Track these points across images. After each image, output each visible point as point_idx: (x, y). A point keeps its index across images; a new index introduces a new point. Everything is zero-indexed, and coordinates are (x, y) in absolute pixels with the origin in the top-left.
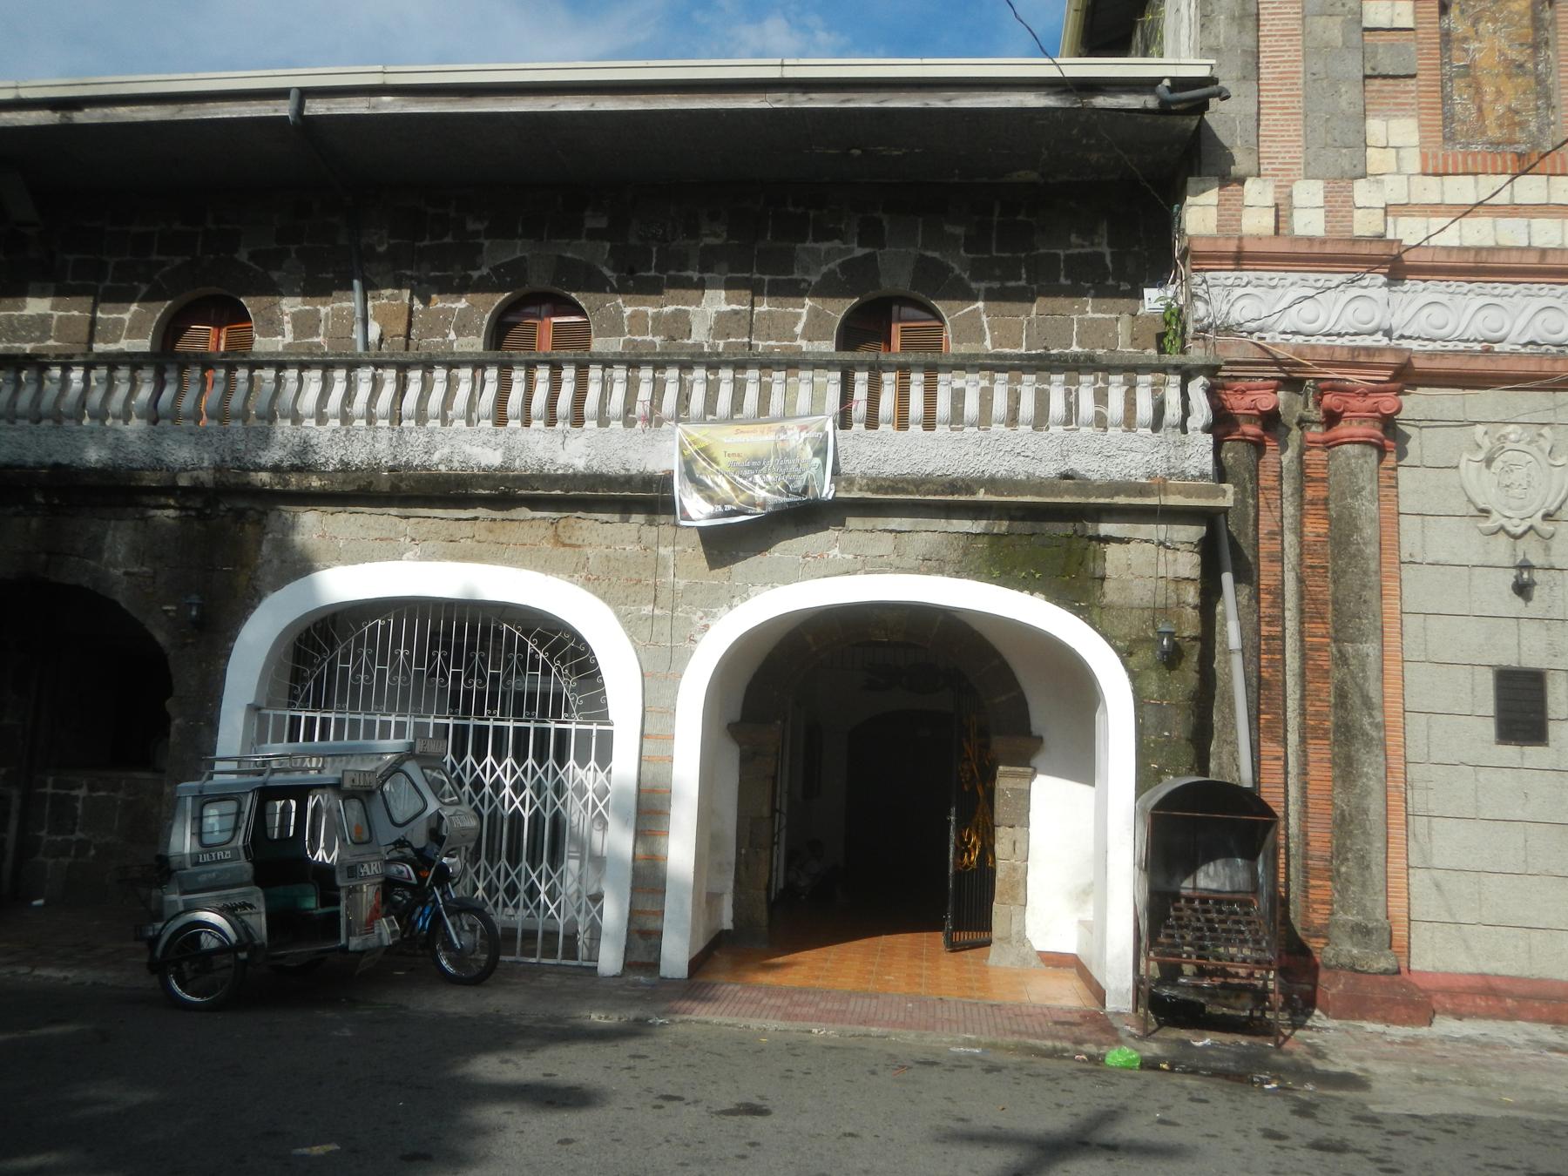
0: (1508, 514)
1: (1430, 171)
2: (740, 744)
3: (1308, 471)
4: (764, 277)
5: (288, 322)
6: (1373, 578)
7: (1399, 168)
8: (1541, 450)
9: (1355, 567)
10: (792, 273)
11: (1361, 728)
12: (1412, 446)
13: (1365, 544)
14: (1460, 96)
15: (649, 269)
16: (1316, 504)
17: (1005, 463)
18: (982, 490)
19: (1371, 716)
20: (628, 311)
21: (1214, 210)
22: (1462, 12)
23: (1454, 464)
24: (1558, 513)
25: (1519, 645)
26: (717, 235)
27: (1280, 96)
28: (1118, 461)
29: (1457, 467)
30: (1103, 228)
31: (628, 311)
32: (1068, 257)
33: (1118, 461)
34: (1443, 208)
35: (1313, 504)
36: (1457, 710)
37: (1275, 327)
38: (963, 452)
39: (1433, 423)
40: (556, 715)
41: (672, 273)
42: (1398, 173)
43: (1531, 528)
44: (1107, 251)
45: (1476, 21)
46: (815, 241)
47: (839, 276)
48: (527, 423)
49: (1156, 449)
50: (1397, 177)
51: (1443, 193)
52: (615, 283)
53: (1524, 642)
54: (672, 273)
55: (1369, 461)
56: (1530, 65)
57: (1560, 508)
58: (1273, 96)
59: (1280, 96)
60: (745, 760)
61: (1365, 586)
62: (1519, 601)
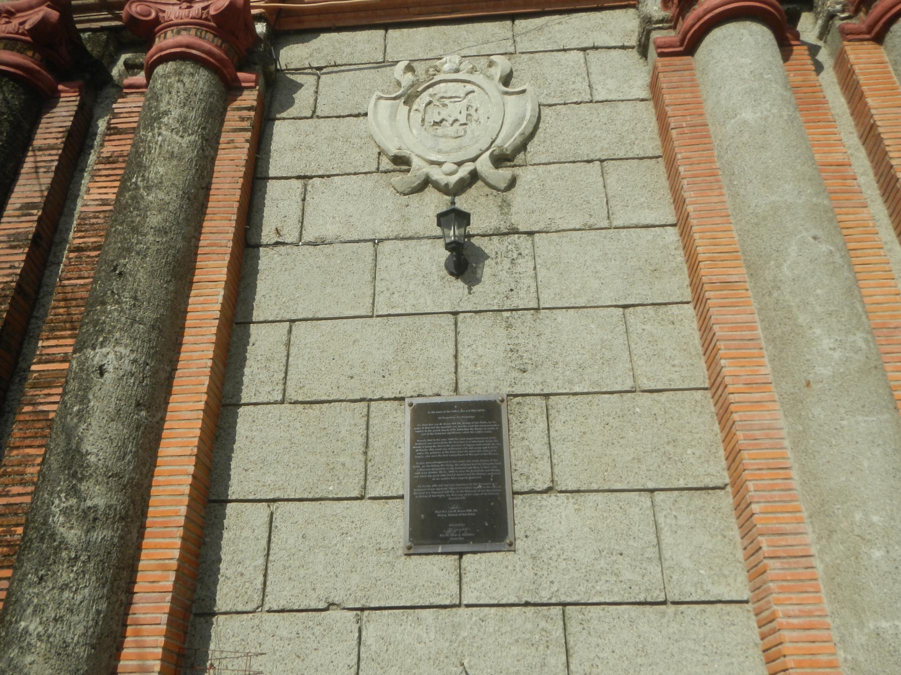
0: (434, 157)
3: (113, 121)
6: (150, 238)
8: (490, 77)
9: (121, 224)
11: (45, 523)
12: (303, 99)
13: (148, 188)
16: (114, 163)
19: (74, 491)
23: (362, 112)
24: (521, 156)
25: (456, 357)
29: (366, 114)
35: (110, 163)
36: (332, 489)
39: (336, 67)
43: (474, 176)
53: (464, 352)
55: (186, 80)
57: (522, 147)
61: (129, 250)
62: (459, 286)
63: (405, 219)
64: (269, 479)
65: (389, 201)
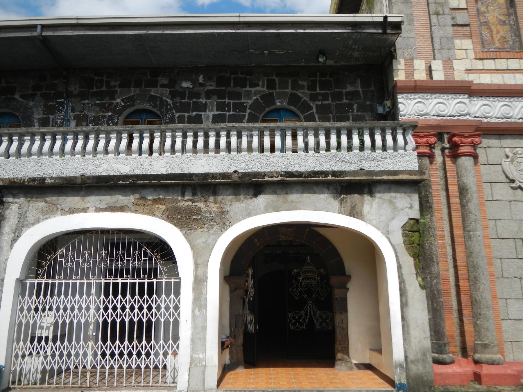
1: (478, 58)
2: (230, 285)
4: (230, 101)
5: (36, 122)
7: (467, 56)
10: (241, 99)
14: (485, 32)
15: (185, 99)
17: (337, 165)
18: (330, 176)
20: (177, 115)
21: (403, 71)
22: (482, 3)
26: (212, 86)
27: (422, 32)
28: (381, 163)
30: (359, 81)
31: (177, 115)
32: (346, 92)
33: (381, 163)
34: (484, 71)
36: (511, 256)
37: (430, 114)
38: (320, 161)
40: (156, 276)
41: (194, 100)
42: (467, 58)
44: (360, 89)
45: (487, 7)
46: (250, 87)
47: (260, 100)
48: (140, 154)
49: (396, 158)
50: (467, 60)
51: (483, 65)
52: (172, 105)
54: (194, 100)
56: (507, 22)
58: (420, 32)
59: (422, 32)
60: (231, 292)
63: (515, 196)
64: (499, 254)
65: (511, 191)
